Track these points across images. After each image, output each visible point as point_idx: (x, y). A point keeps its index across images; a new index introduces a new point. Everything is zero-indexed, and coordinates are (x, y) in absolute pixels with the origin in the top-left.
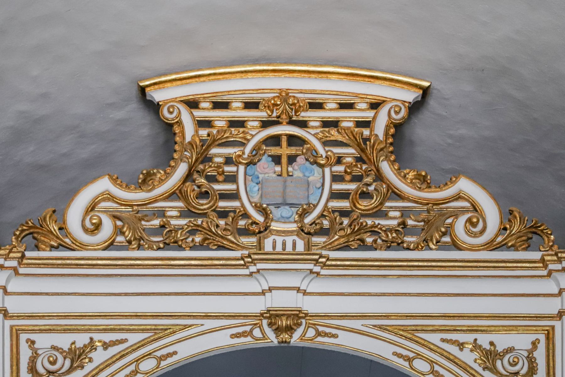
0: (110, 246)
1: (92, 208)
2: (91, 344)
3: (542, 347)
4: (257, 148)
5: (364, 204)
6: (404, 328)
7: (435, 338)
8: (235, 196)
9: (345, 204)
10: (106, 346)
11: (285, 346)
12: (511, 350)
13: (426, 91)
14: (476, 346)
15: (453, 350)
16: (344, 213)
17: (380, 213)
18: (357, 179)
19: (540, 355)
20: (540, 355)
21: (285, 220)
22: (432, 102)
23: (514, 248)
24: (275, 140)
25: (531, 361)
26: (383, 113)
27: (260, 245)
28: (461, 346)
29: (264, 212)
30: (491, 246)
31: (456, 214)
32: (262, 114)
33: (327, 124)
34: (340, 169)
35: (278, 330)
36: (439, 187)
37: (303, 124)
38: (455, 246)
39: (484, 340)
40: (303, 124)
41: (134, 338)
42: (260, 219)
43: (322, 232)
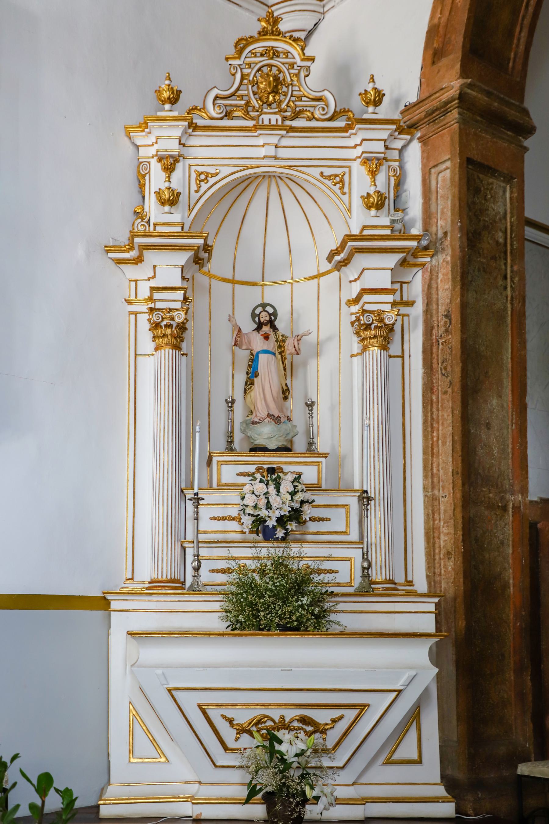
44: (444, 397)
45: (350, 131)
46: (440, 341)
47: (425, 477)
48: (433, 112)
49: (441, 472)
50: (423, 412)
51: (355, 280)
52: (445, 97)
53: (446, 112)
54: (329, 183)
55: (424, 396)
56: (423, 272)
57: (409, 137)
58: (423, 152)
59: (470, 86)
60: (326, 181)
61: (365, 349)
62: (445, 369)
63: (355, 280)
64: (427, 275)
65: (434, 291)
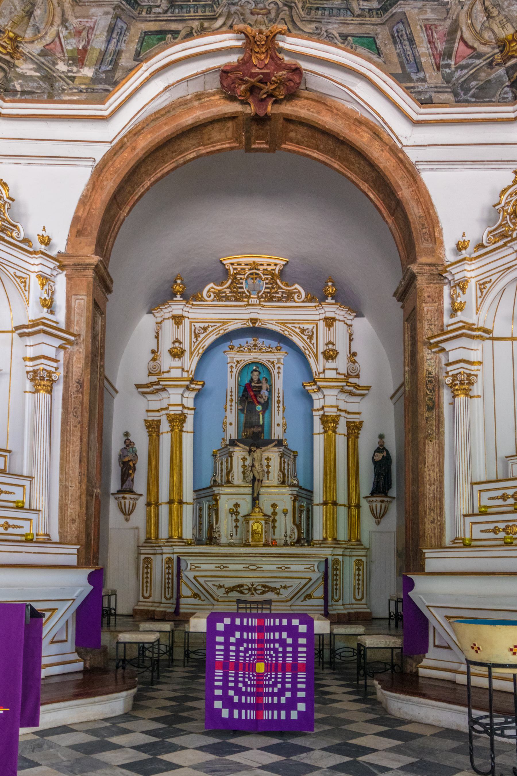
0: (213, 300)
1: (208, 291)
2: (208, 327)
3: (315, 328)
4: (248, 276)
5: (273, 290)
6: (282, 323)
7: (289, 326)
8: (242, 288)
9: (268, 290)
10: (212, 326)
11: (254, 327)
12: (307, 329)
13: (287, 262)
14: (299, 328)
15: (294, 329)
16: (268, 293)
17: (276, 293)
18: (271, 284)
19: (315, 330)
20: (315, 330)
21: (254, 294)
22: (289, 263)
23: (309, 302)
24: (252, 274)
25: (312, 332)
26: (278, 266)
27: (248, 302)
28: (296, 328)
29: (249, 292)
30: (303, 302)
31: (295, 293)
32: (249, 267)
33: (264, 269)
34: (267, 281)
35: (252, 323)
36: (291, 286)
37: (259, 270)
38: (294, 301)
39: (301, 326)
40: (259, 270)
41: (218, 325)
42: (248, 294)
43: (262, 297)
44: (75, 429)
45: (34, 255)
46: (73, 396)
47: (61, 473)
48: (79, 265)
49: (71, 472)
50: (61, 435)
51: (30, 346)
52: (88, 261)
53: (85, 269)
54: (18, 280)
55: (62, 425)
56: (65, 353)
57: (61, 271)
58: (67, 283)
59: (101, 261)
60: (17, 279)
61: (37, 391)
62: (76, 413)
63: (30, 346)
64: (67, 355)
65: (70, 366)
